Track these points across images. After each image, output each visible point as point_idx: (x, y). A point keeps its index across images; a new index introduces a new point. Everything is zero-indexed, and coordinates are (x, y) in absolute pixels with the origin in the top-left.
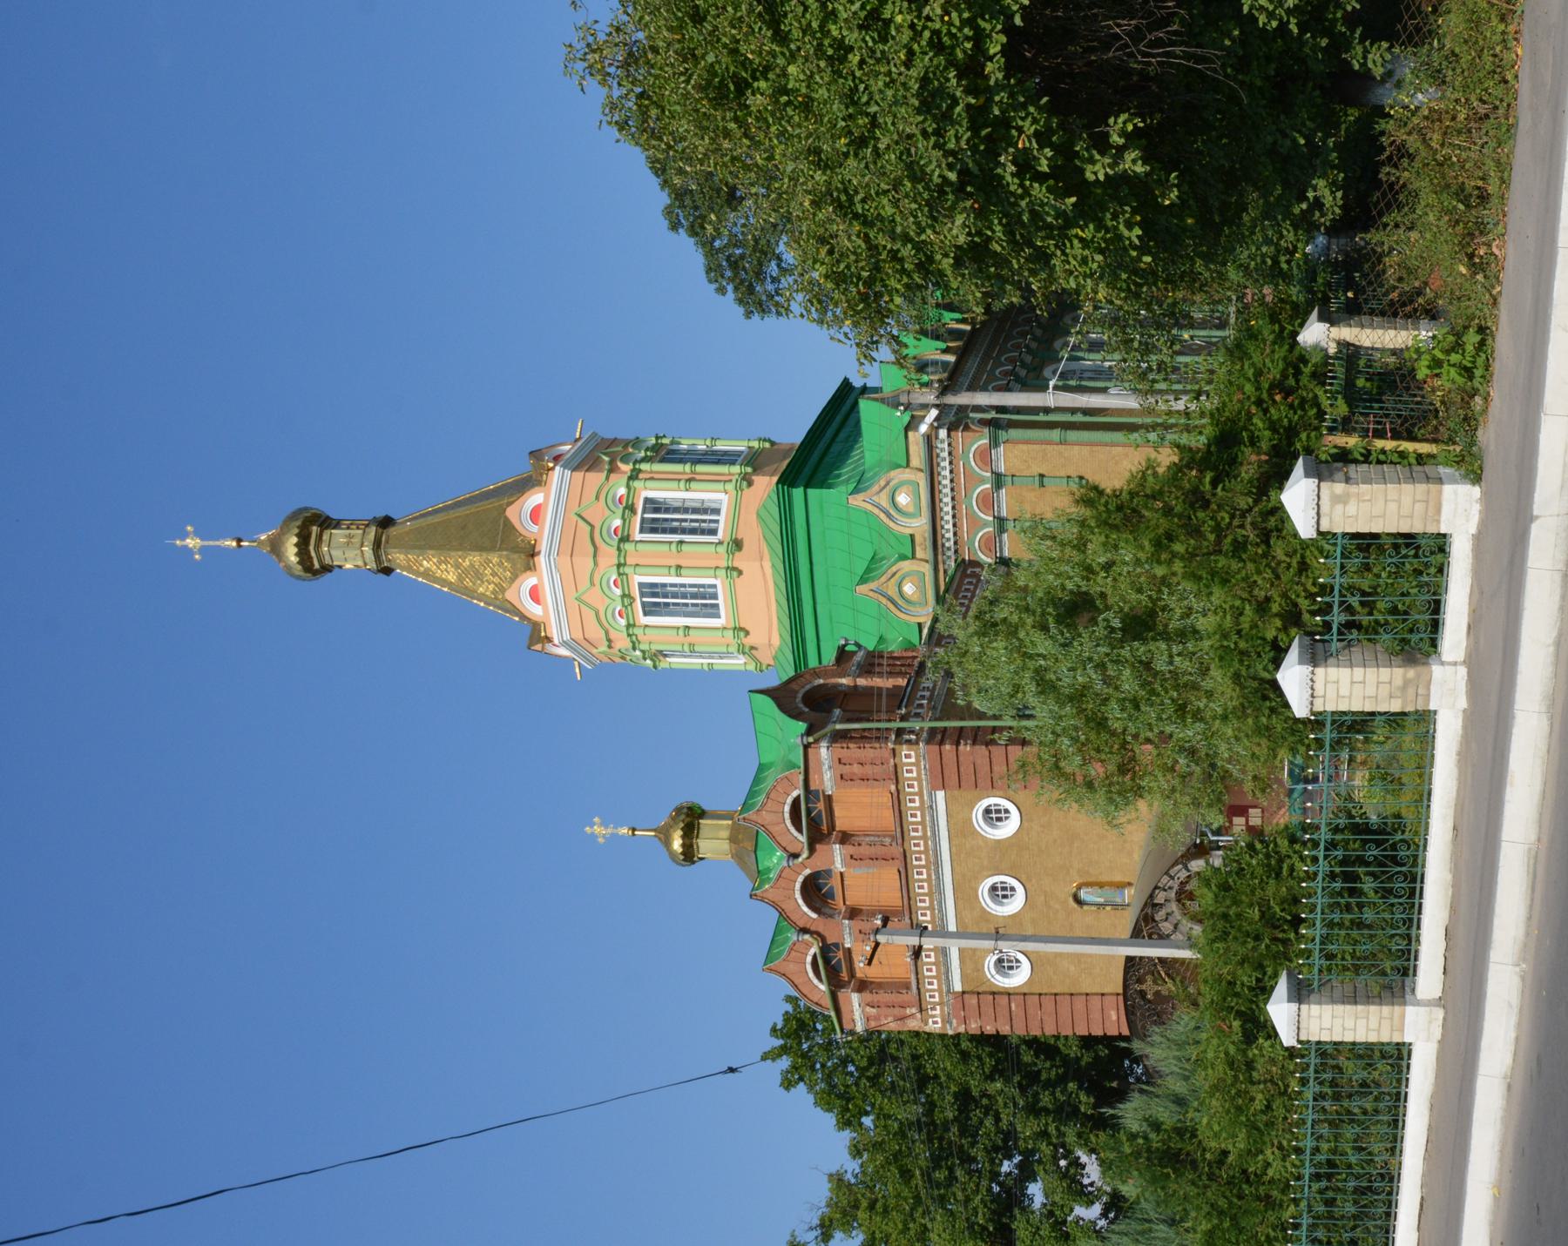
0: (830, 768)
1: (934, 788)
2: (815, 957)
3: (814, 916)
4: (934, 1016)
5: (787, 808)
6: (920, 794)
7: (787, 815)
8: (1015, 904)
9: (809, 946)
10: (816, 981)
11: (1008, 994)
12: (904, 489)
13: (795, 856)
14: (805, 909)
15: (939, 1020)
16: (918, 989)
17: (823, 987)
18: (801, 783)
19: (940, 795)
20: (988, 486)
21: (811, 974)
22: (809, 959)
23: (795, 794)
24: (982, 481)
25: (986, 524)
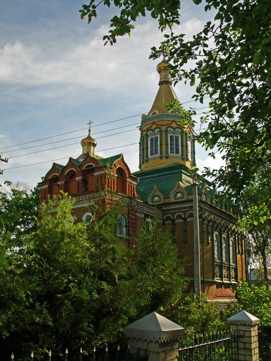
0: (100, 174)
2: (56, 175)
3: (66, 174)
7: (89, 164)
9: (59, 174)
10: (51, 176)
12: (182, 195)
13: (79, 167)
14: (67, 171)
17: (50, 178)
18: (96, 166)
20: (183, 217)
21: (53, 175)
22: (56, 174)
23: (94, 166)
24: (185, 215)
25: (173, 217)
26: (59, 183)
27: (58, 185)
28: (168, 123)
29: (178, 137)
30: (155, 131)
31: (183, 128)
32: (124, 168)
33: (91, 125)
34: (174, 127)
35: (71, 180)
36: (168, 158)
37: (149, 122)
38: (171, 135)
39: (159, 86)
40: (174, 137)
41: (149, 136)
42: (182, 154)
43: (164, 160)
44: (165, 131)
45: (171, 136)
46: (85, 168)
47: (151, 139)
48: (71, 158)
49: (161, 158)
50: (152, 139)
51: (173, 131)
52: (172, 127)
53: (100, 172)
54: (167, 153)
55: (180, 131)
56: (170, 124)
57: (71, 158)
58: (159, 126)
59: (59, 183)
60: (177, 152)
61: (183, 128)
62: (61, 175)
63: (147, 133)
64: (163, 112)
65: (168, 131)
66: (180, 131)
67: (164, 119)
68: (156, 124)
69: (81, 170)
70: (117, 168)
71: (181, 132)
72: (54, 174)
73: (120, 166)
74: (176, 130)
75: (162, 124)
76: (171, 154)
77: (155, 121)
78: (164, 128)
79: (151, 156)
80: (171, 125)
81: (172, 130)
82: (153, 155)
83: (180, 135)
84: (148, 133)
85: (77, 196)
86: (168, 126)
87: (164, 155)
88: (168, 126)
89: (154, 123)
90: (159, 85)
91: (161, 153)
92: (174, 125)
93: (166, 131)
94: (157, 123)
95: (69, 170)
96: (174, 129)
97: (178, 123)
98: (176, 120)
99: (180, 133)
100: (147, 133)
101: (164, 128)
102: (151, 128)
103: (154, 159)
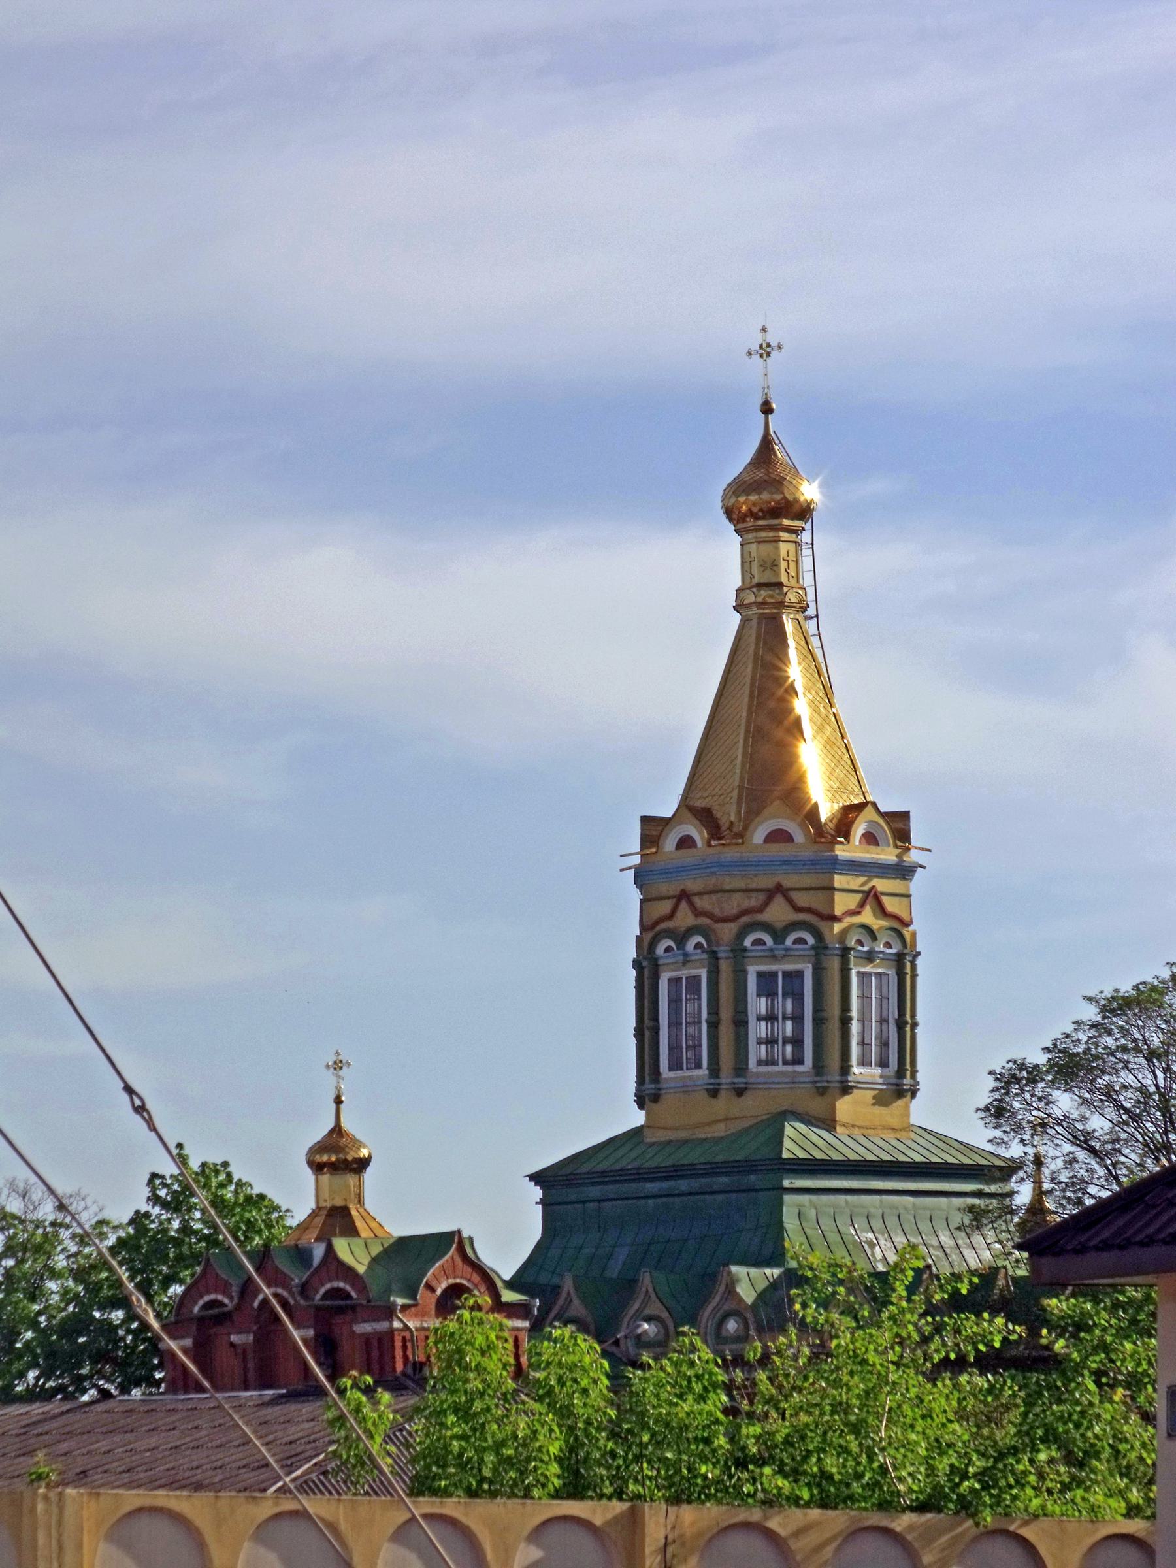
3: (256, 1304)
10: (201, 1303)
31: (822, 926)
32: (469, 1280)
33: (341, 1073)
36: (748, 1093)
42: (819, 1066)
43: (723, 1105)
45: (760, 975)
49: (714, 1093)
50: (675, 982)
51: (771, 950)
52: (766, 927)
56: (761, 910)
61: (822, 926)
62: (238, 1307)
66: (811, 940)
67: (729, 883)
68: (692, 905)
69: (309, 1306)
70: (439, 1292)
73: (451, 1281)
77: (692, 885)
83: (810, 966)
86: (745, 919)
88: (745, 919)
91: (715, 1070)
93: (739, 953)
96: (779, 935)
98: (787, 882)
101: (727, 931)
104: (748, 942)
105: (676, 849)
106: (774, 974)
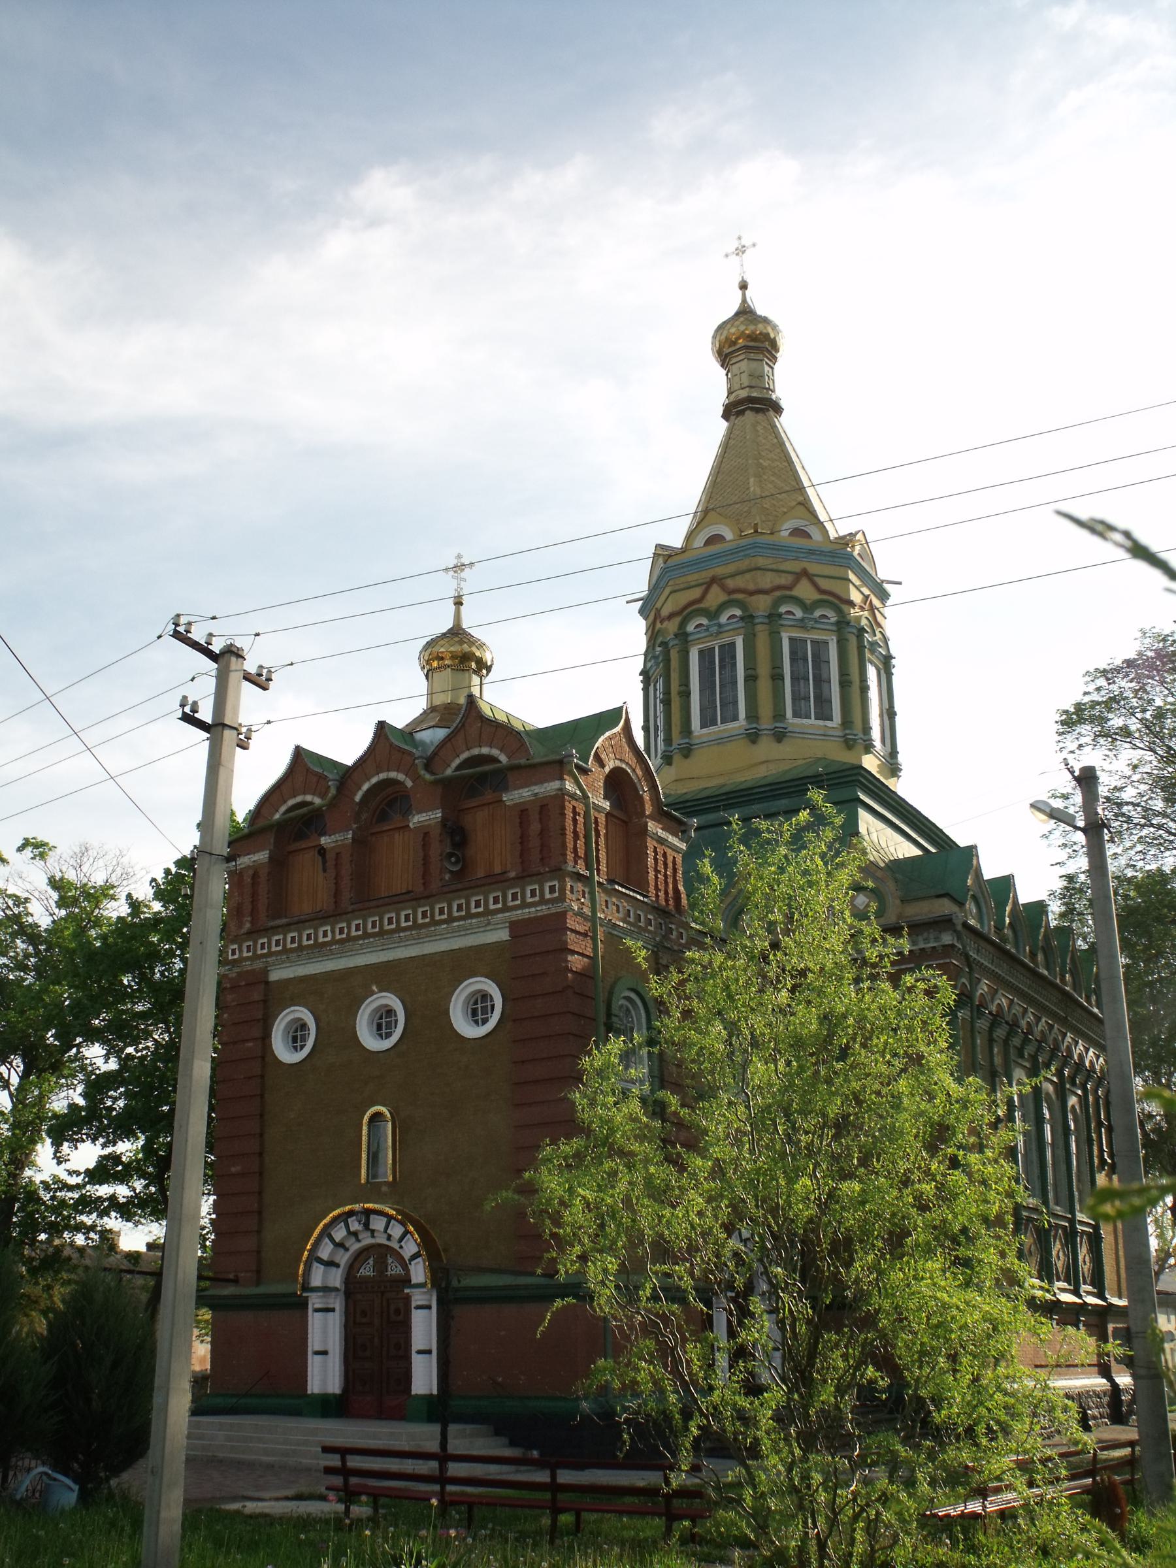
0: (535, 795)
1: (514, 926)
2: (311, 803)
3: (358, 798)
4: (241, 951)
5: (485, 750)
6: (506, 909)
8: (370, 1041)
9: (322, 796)
10: (283, 809)
11: (266, 1037)
13: (428, 767)
14: (366, 787)
15: (236, 957)
16: (272, 928)
17: (277, 816)
19: (503, 935)
21: (291, 802)
22: (309, 798)
23: (503, 758)
26: (323, 840)
27: (322, 851)
28: (783, 580)
29: (826, 643)
30: (723, 619)
31: (844, 607)
32: (634, 770)
33: (463, 575)
34: (808, 602)
35: (385, 829)
36: (785, 740)
37: (693, 578)
38: (797, 634)
39: (724, 425)
40: (809, 642)
41: (691, 638)
42: (846, 723)
43: (766, 748)
44: (770, 616)
46: (458, 768)
47: (701, 652)
48: (382, 726)
49: (753, 737)
50: (706, 656)
51: (802, 620)
53: (537, 789)
54: (779, 716)
55: (833, 617)
56: (790, 588)
57: (382, 726)
58: (740, 596)
59: (323, 840)
60: (824, 713)
61: (844, 607)
62: (333, 804)
63: (683, 624)
64: (756, 531)
65: (780, 616)
66: (833, 617)
67: (761, 562)
68: (723, 588)
69: (436, 783)
70: (607, 770)
71: (838, 623)
72: (299, 799)
73: (618, 763)
74: (817, 613)
75: (751, 587)
76: (797, 721)
77: (720, 571)
78: (762, 604)
79: (705, 731)
80: (795, 593)
81: (799, 614)
82: (713, 722)
83: (835, 638)
84: (690, 628)
85: (422, 901)
86: (778, 594)
87: (766, 723)
88: (778, 594)
89: (713, 580)
90: (726, 415)
91: (752, 716)
92: (804, 591)
93: (773, 617)
94: (731, 583)
95: (374, 780)
96: (807, 608)
97: (824, 584)
98: (813, 568)
99: (834, 628)
100: (683, 624)
101: (762, 604)
102: (702, 605)
103: (721, 741)
104: (783, 609)
105: (705, 545)
106: (804, 641)
